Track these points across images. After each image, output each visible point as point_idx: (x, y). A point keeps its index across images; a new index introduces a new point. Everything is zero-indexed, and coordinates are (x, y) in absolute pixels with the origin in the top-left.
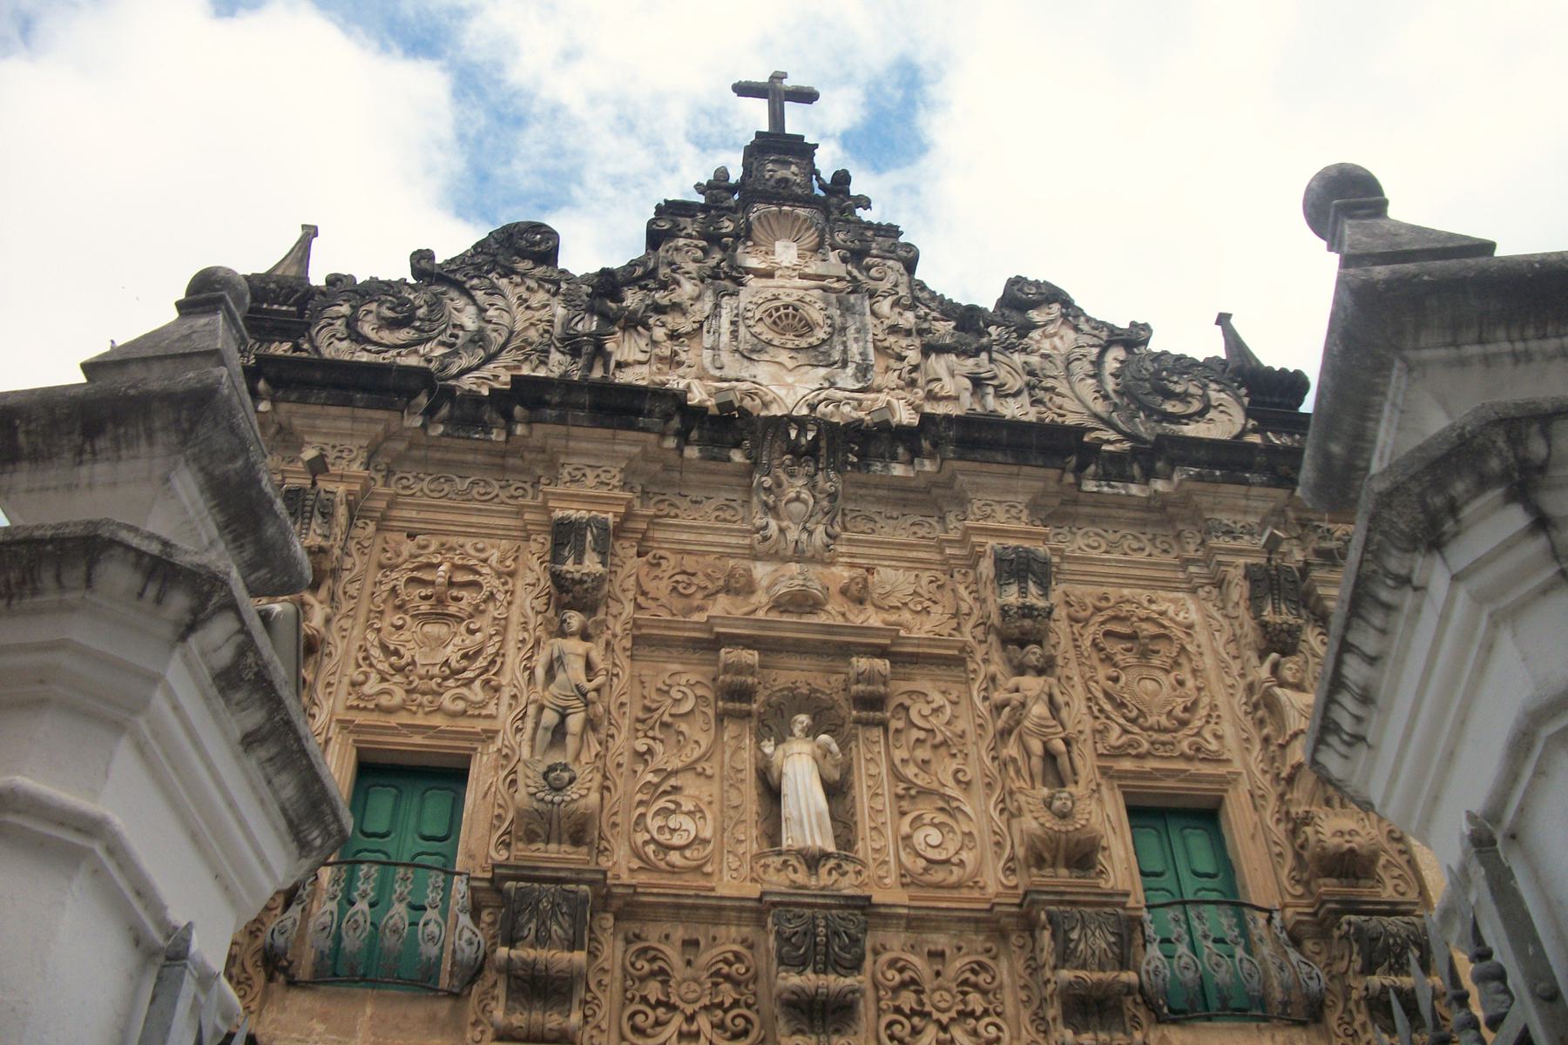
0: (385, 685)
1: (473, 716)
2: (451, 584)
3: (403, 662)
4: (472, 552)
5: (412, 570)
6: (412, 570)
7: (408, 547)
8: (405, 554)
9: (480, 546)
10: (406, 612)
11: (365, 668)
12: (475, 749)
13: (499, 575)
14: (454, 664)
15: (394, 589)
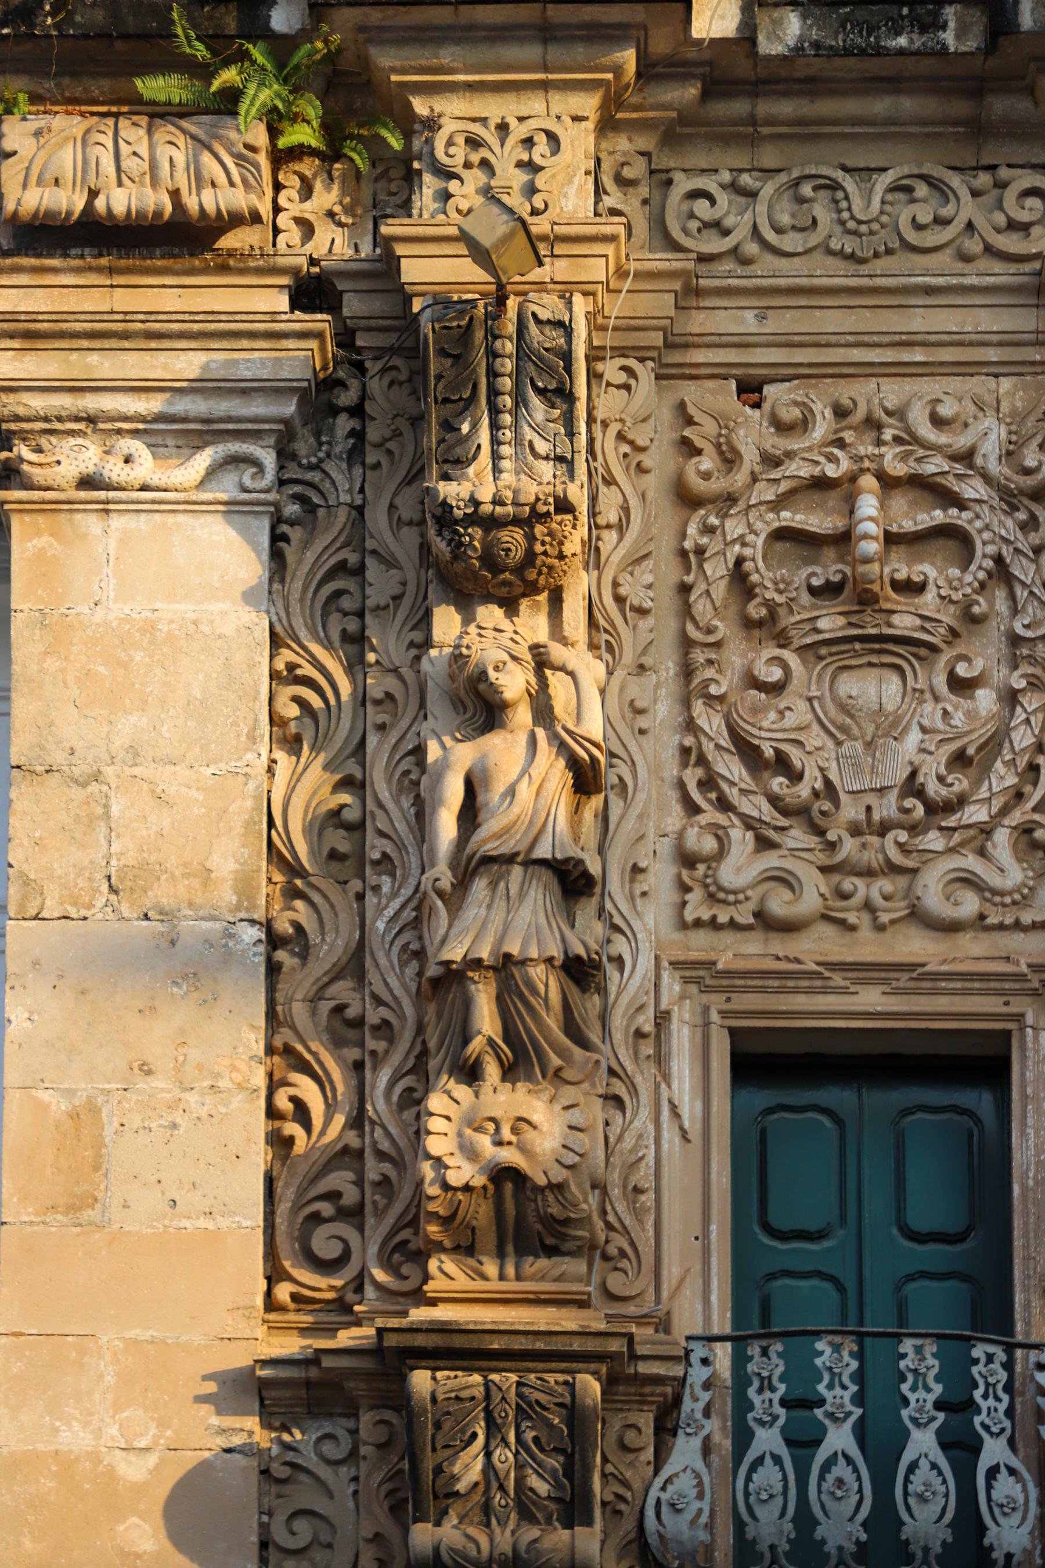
0: (771, 860)
1: (1001, 927)
2: (890, 539)
3: (804, 791)
4: (926, 431)
5: (777, 505)
6: (777, 505)
7: (752, 434)
8: (750, 456)
9: (945, 410)
10: (782, 640)
11: (711, 815)
12: (1019, 1017)
13: (1010, 499)
14: (933, 788)
15: (739, 575)
